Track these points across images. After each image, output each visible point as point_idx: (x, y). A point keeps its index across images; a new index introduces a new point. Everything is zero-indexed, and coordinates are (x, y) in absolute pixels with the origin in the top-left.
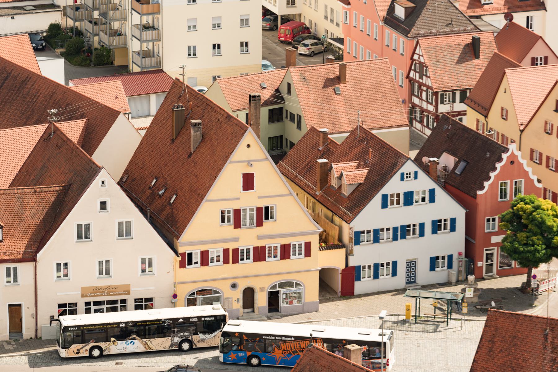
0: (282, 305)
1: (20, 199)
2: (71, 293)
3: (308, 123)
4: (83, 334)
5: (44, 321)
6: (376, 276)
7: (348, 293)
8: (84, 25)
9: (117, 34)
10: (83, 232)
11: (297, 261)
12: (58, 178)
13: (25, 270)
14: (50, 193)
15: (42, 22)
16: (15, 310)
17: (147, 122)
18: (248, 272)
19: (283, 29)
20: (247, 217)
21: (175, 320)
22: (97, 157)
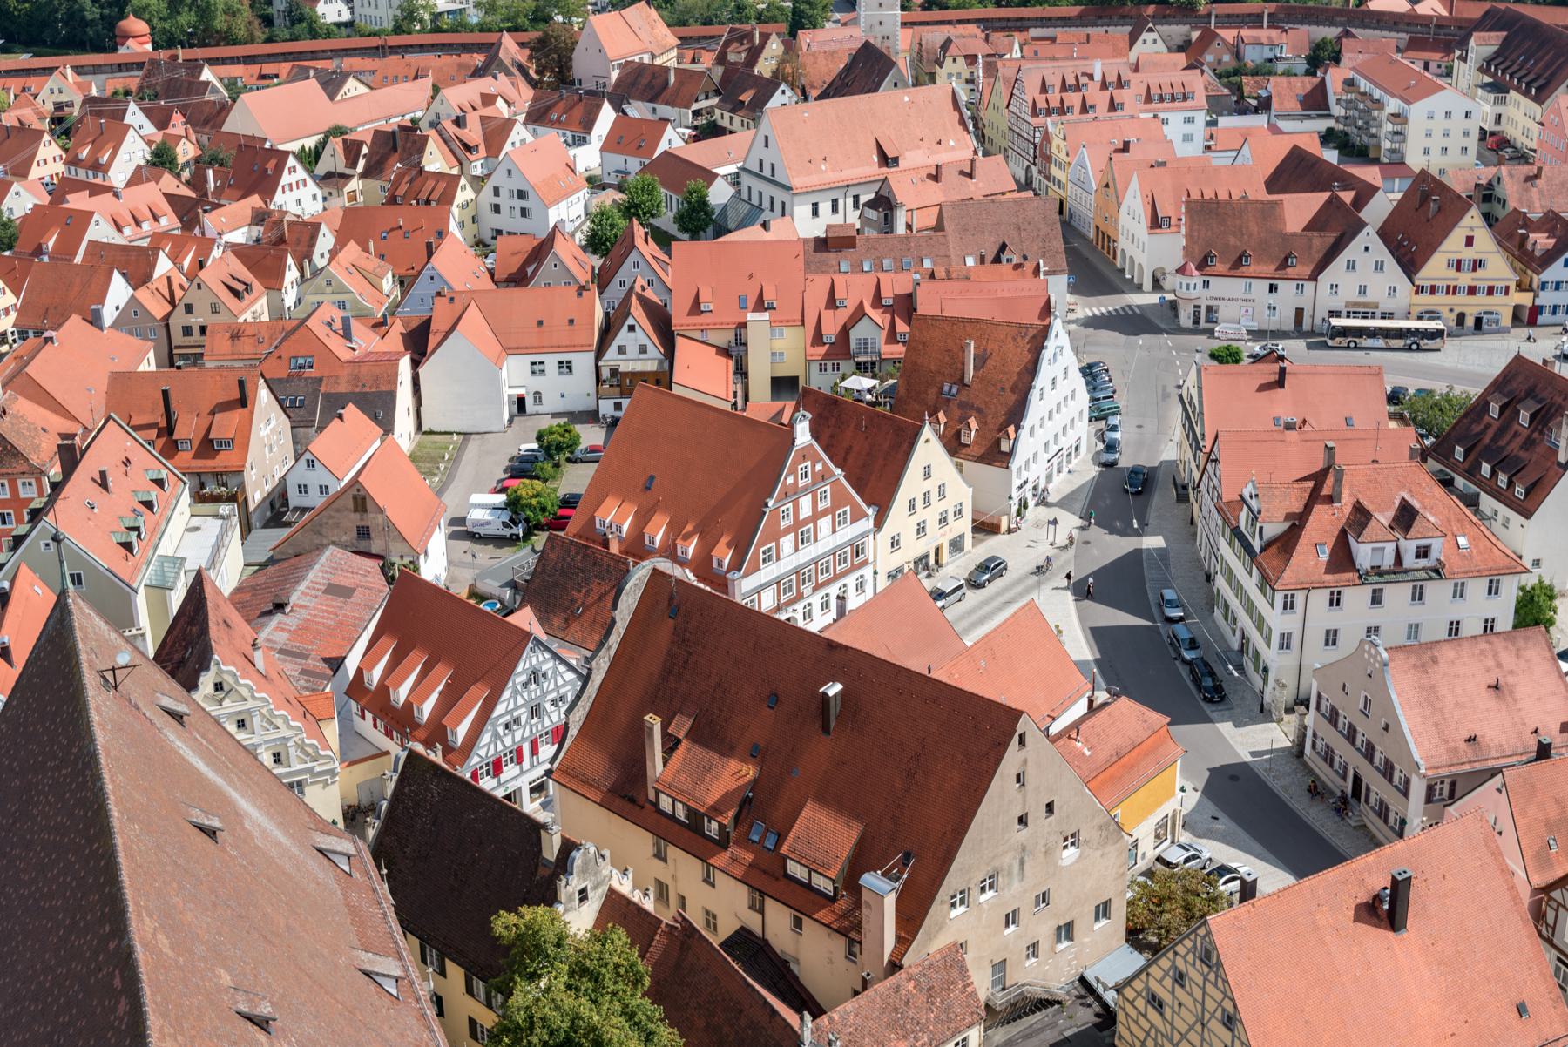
0: (1484, 326)
1: (1310, 239)
2: (1338, 303)
3: (1512, 204)
4: (1345, 332)
5: (1318, 321)
6: (1554, 313)
7: (1532, 322)
8: (1351, 130)
9: (1373, 136)
10: (1351, 266)
11: (1498, 298)
12: (1337, 227)
13: (1309, 286)
14: (1331, 236)
15: (1323, 125)
16: (1299, 312)
17: (1399, 196)
18: (1462, 301)
19: (1490, 140)
20: (1466, 265)
21: (1409, 330)
22: (1362, 215)
